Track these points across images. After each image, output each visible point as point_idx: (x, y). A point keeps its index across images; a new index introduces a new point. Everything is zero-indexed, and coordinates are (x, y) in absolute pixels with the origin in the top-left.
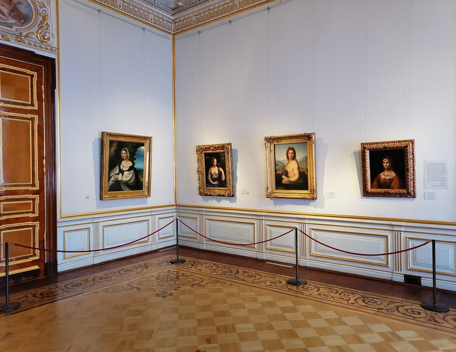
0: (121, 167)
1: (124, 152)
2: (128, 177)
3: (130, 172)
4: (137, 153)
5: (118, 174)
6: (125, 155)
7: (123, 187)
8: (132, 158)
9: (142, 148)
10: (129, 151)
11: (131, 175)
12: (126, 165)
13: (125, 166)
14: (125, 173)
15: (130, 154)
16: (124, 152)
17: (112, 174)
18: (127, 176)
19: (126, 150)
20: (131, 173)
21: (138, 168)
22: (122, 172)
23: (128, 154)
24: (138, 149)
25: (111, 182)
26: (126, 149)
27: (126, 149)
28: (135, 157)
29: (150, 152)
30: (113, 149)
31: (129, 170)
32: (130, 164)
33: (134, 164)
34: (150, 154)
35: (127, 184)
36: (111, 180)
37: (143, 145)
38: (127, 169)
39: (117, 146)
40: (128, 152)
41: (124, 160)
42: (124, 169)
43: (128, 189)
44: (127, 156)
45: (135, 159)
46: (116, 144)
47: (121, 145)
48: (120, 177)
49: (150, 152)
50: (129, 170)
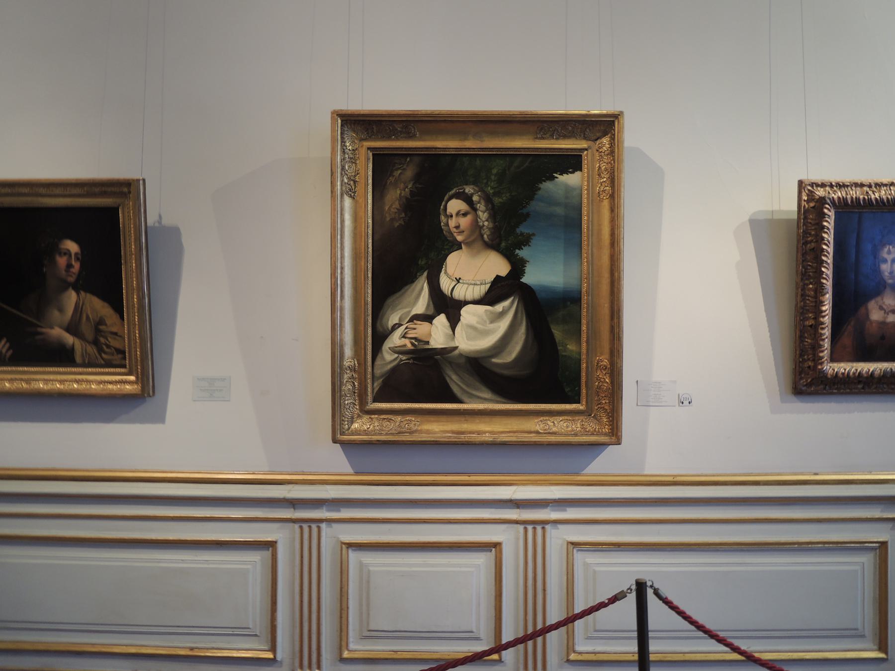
0: (445, 284)
1: (455, 205)
2: (485, 333)
3: (499, 307)
4: (535, 206)
5: (428, 318)
6: (465, 222)
7: (455, 381)
8: (507, 235)
9: (571, 179)
10: (488, 200)
11: (503, 325)
12: (470, 271)
13: (466, 277)
14: (469, 314)
15: (493, 217)
16: (455, 205)
17: (393, 319)
18: (481, 330)
19: (468, 200)
20: (502, 314)
21: (546, 289)
22: (448, 306)
23: (483, 216)
24: (547, 186)
25: (388, 357)
26: (469, 190)
27: (469, 190)
28: (523, 229)
29: (612, 197)
30: (394, 197)
31: (490, 298)
32: (496, 266)
33: (518, 267)
34: (612, 210)
35: (478, 368)
36: (389, 344)
37: (572, 162)
38: (479, 291)
39: (417, 178)
40: (481, 207)
41: (458, 246)
42: (460, 293)
43: (487, 395)
44: (476, 226)
45: (525, 241)
46: (409, 173)
47: (438, 176)
48: (438, 333)
49: (612, 197)
50: (490, 298)
